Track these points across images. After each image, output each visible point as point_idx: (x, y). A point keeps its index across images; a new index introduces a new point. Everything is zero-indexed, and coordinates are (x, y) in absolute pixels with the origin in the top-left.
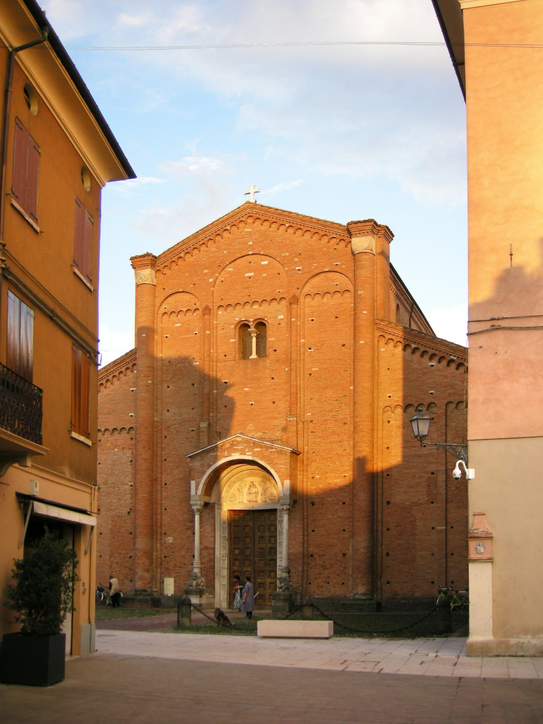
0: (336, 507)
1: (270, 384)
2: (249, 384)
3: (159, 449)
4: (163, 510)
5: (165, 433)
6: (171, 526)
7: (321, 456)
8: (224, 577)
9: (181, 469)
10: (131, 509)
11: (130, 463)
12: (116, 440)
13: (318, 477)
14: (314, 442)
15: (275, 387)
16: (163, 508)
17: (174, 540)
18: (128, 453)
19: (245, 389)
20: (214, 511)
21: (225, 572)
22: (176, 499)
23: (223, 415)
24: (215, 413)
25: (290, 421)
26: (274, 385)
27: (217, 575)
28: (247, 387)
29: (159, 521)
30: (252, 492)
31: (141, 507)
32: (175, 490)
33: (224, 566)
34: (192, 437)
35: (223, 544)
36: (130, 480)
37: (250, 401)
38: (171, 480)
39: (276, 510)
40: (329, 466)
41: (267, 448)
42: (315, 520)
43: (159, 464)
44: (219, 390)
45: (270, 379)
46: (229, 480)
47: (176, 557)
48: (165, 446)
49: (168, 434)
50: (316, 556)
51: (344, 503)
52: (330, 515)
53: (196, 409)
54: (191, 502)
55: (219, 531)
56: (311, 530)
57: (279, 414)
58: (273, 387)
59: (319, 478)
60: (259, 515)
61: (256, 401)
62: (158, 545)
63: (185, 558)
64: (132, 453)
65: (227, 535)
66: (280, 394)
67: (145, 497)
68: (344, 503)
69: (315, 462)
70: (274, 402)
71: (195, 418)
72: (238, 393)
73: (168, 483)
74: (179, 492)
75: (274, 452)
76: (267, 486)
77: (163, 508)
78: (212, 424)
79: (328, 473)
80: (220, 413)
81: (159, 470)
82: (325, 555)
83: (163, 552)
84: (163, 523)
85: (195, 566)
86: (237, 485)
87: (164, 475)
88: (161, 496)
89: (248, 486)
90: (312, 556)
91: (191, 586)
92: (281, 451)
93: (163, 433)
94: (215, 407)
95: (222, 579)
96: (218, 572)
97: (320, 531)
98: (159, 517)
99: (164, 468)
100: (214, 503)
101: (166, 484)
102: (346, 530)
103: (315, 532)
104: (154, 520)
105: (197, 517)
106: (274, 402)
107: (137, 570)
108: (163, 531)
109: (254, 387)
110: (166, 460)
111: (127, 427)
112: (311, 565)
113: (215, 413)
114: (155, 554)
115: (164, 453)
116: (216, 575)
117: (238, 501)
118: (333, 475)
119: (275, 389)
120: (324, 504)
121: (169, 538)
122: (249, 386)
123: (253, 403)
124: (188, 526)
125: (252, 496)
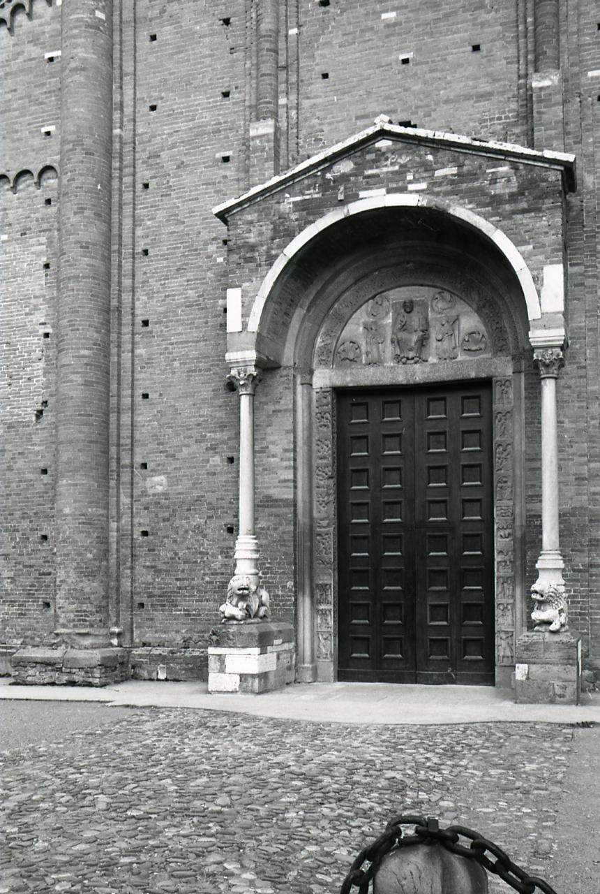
3: (127, 223)
4: (139, 399)
5: (144, 174)
9: (190, 275)
10: (45, 403)
11: (42, 272)
12: (5, 209)
16: (139, 392)
18: (38, 246)
19: (384, 16)
22: (176, 364)
23: (318, 101)
24: (293, 97)
29: (126, 433)
31: (75, 389)
32: (173, 340)
36: (42, 320)
37: (401, 50)
43: (127, 266)
44: (302, 29)
48: (144, 212)
49: (151, 178)
62: (125, 500)
63: (205, 536)
64: (50, 243)
67: (84, 357)
70: (476, 48)
77: (139, 392)
81: (127, 282)
83: (136, 521)
84: (137, 436)
87: (142, 297)
88: (133, 360)
93: (138, 175)
94: (293, 79)
98: (126, 419)
99: (140, 277)
104: (113, 427)
106: (476, 48)
107: (61, 574)
108: (139, 460)
110: (146, 252)
111: (36, 168)
114: (114, 525)
115: (139, 232)
121: (157, 479)
123: (409, 55)
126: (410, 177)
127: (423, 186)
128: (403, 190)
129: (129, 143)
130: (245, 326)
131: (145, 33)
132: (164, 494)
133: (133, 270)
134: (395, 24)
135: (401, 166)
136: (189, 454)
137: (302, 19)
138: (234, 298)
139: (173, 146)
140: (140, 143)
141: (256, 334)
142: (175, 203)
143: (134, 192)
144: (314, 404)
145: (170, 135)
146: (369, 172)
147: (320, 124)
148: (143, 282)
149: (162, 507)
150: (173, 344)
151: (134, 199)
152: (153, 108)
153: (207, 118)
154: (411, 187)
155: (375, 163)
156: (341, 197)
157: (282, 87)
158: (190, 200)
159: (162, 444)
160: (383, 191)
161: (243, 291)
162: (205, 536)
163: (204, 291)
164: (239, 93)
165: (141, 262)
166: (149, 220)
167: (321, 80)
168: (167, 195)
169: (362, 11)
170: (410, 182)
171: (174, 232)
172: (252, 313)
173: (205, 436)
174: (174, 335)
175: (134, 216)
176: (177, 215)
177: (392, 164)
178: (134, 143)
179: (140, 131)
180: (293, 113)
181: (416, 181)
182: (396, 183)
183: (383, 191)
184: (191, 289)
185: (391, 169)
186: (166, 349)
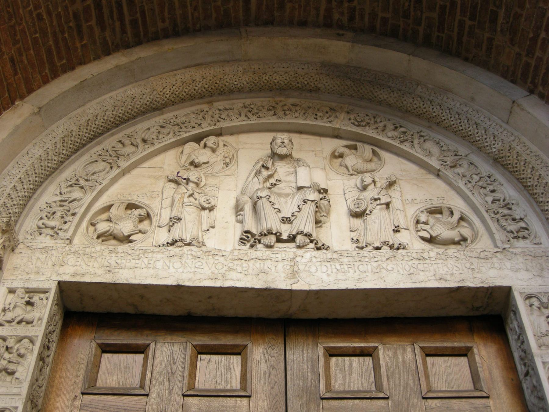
60: (332, 353)
117: (163, 236)
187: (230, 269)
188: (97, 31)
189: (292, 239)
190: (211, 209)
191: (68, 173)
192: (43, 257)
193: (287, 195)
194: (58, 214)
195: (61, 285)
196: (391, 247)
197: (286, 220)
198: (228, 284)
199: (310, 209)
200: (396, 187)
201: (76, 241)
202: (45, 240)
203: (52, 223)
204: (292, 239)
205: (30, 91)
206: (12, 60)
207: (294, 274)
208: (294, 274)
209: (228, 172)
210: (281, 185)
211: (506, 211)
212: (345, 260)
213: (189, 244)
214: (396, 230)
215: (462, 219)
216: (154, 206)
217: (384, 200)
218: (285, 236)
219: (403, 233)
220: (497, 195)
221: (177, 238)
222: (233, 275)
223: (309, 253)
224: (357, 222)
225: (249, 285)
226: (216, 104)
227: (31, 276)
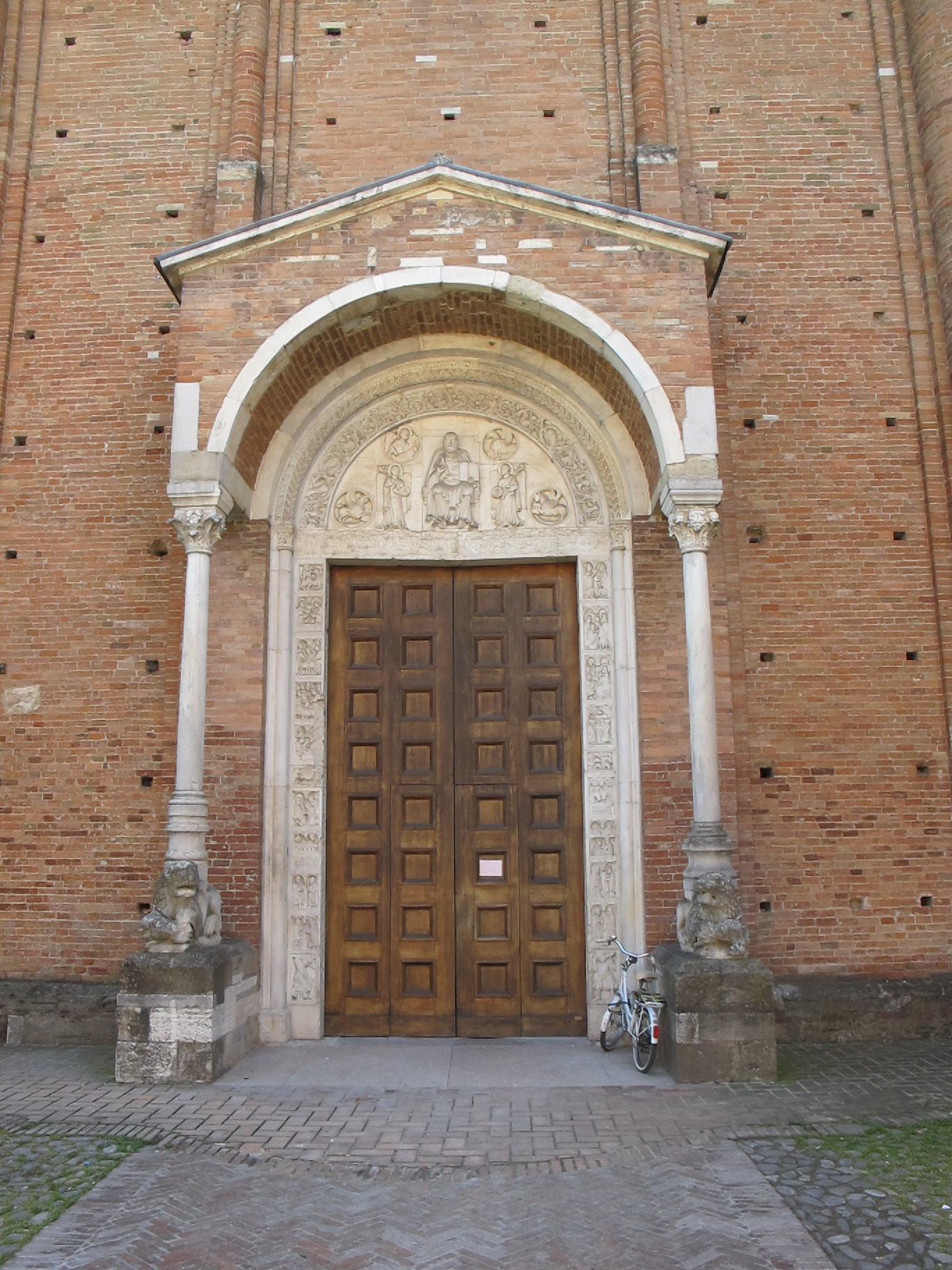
0: (868, 552)
1: (532, 43)
2: (439, 39)
5: (37, 222)
6: (36, 633)
7: (778, 332)
8: (300, 880)
9: (103, 374)
13: (775, 417)
14: (741, 273)
15: (553, 55)
17: (46, 699)
19: (419, 59)
20: (266, 556)
21: (312, 859)
22: (69, 507)
23: (317, 152)
25: (650, 167)
26: (545, 49)
27: (274, 867)
28: (431, 53)
30: (451, 482)
32: (67, 469)
33: (304, 830)
34: (169, 238)
35: (299, 722)
37: (443, 103)
38: (50, 421)
39: (569, 565)
40: (815, 374)
41: (587, 238)
42: (774, 607)
45: (532, 24)
46: (341, 423)
47: (52, 782)
48: (35, 276)
49: (51, 228)
50: (786, 775)
51: (899, 536)
52: (843, 586)
53: (192, 131)
54: (171, 489)
55: (284, 656)
56: (757, 655)
57: (574, 158)
58: (544, 55)
59: (778, 423)
61: (467, 105)
63: (102, 789)
65: (321, 679)
66: (577, 84)
68: (899, 536)
69: (749, 357)
70: (549, 114)
71: (186, 165)
72: (388, 72)
73: (33, 435)
74: (89, 474)
75: (623, 257)
76: (518, 458)
78: (268, 180)
79: (815, 404)
80: (304, 146)
82: (831, 772)
85: (174, 825)
86: (375, 451)
89: (427, 455)
90: (766, 773)
91: (164, 938)
92: (660, 252)
93: (29, 223)
94: (285, 118)
95: (293, 890)
96: (280, 857)
97: (800, 657)
99: (17, 368)
100: (267, 523)
101: (21, 441)
102: (921, 652)
103: (776, 661)
105: (197, 568)
109: (462, 51)
112: (766, 819)
113: (283, 140)
115: (23, 304)
116: (267, 869)
117: (380, 519)
118: (839, 413)
119: (553, 65)
120: (809, 537)
121: (22, 691)
122: (439, 46)
123: (456, 111)
124: (128, 630)
125: (454, 497)
126: (481, 244)
127: (501, 259)
128: (473, 262)
129: (19, 176)
130: (202, 444)
131: (59, 33)
132: (32, 715)
133: (8, 358)
134: (434, 71)
135: (467, 230)
136: (82, 652)
137: (301, 47)
138: (187, 396)
139: (89, 188)
140: (36, 179)
141: (220, 458)
142: (86, 267)
143: (20, 244)
144: (296, 586)
145: (86, 173)
146: (417, 232)
147: (321, 182)
148: (22, 378)
149: (29, 739)
150: (64, 475)
151: (19, 255)
152: (62, 134)
153: (143, 156)
154: (482, 259)
155: (424, 222)
156: (371, 262)
157: (269, 125)
158: (111, 265)
159: (36, 633)
160: (439, 260)
161: (201, 388)
162: (102, 789)
163: (124, 398)
164: (200, 128)
165: (23, 349)
166: (42, 287)
167: (325, 126)
168: (72, 255)
169: (389, 49)
170: (482, 252)
171: (81, 309)
172: (216, 424)
173: (111, 624)
174: (67, 462)
175: (16, 279)
176: (89, 285)
177: (453, 225)
178: (27, 177)
179: (38, 161)
180: (283, 161)
181: (490, 251)
182: (461, 252)
183: (439, 260)
184: (103, 394)
185: (451, 231)
186: (52, 482)
187: (421, 547)
188: (319, 370)
189: (456, 523)
190: (408, 495)
191: (314, 470)
192: (313, 541)
193: (452, 487)
194: (316, 506)
195: (328, 560)
196: (514, 525)
197: (452, 508)
198: (420, 557)
199: (466, 501)
200: (523, 473)
201: (330, 526)
202: (311, 529)
203: (313, 514)
204: (456, 523)
205: (282, 420)
206: (272, 417)
207: (456, 550)
208: (456, 550)
209: (416, 460)
210: (450, 478)
211: (587, 496)
212: (485, 538)
213: (396, 527)
214: (519, 511)
215: (562, 496)
216: (372, 492)
217: (513, 488)
218: (452, 521)
219: (524, 512)
220: (585, 482)
221: (389, 522)
222: (422, 551)
223: (465, 535)
224: (497, 501)
225: (431, 558)
226: (405, 393)
227: (310, 556)
